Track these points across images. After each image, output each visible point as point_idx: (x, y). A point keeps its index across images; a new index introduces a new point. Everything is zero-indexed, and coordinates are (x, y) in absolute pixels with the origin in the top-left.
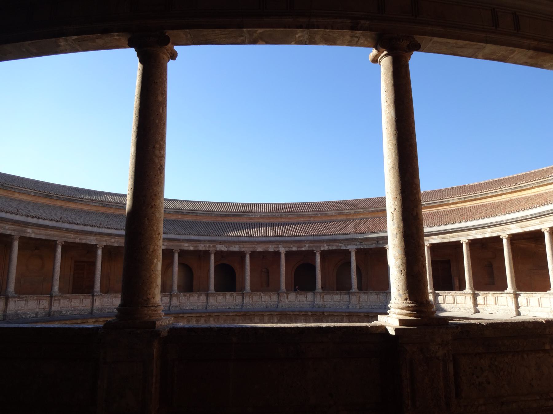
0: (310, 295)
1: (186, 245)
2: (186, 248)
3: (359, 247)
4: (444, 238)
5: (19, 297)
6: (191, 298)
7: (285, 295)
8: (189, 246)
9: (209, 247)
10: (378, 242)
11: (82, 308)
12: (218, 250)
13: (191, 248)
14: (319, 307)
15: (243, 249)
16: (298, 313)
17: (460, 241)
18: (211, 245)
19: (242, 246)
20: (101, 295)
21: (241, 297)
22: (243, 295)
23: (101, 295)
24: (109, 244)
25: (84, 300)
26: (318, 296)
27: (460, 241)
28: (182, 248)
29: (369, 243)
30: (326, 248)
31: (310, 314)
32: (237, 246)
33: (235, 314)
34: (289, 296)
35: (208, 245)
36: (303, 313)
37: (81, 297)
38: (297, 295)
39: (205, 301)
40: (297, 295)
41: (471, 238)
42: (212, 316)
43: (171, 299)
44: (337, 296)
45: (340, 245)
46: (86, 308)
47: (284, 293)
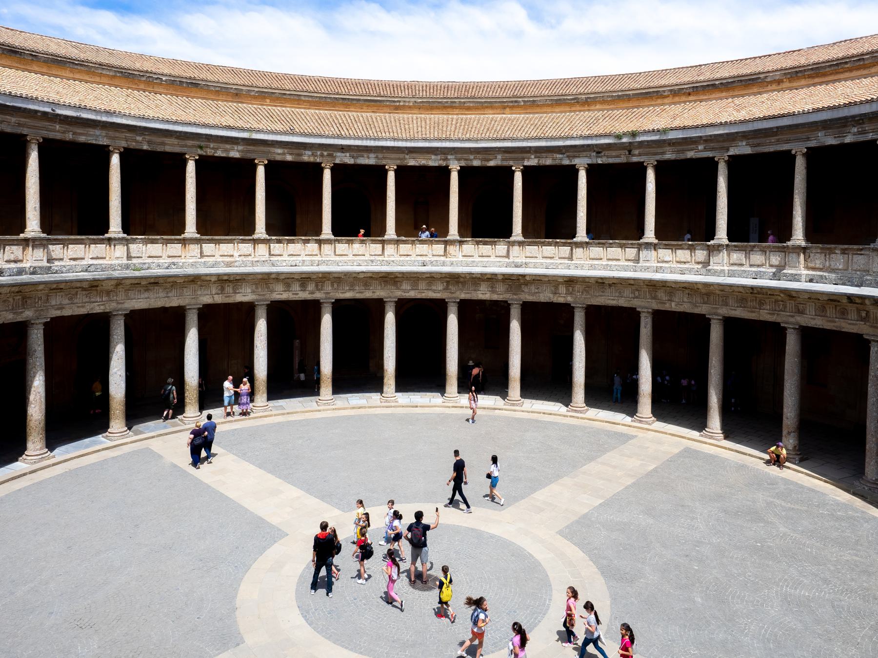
0: (501, 248)
1: (280, 151)
3: (595, 162)
4: (758, 145)
8: (284, 154)
9: (322, 155)
10: (630, 152)
12: (337, 161)
13: (289, 158)
14: (516, 266)
17: (790, 151)
18: (325, 153)
19: (380, 156)
24: (133, 145)
27: (790, 151)
28: (272, 158)
29: (614, 153)
32: (372, 155)
35: (319, 153)
41: (813, 144)
45: (561, 156)
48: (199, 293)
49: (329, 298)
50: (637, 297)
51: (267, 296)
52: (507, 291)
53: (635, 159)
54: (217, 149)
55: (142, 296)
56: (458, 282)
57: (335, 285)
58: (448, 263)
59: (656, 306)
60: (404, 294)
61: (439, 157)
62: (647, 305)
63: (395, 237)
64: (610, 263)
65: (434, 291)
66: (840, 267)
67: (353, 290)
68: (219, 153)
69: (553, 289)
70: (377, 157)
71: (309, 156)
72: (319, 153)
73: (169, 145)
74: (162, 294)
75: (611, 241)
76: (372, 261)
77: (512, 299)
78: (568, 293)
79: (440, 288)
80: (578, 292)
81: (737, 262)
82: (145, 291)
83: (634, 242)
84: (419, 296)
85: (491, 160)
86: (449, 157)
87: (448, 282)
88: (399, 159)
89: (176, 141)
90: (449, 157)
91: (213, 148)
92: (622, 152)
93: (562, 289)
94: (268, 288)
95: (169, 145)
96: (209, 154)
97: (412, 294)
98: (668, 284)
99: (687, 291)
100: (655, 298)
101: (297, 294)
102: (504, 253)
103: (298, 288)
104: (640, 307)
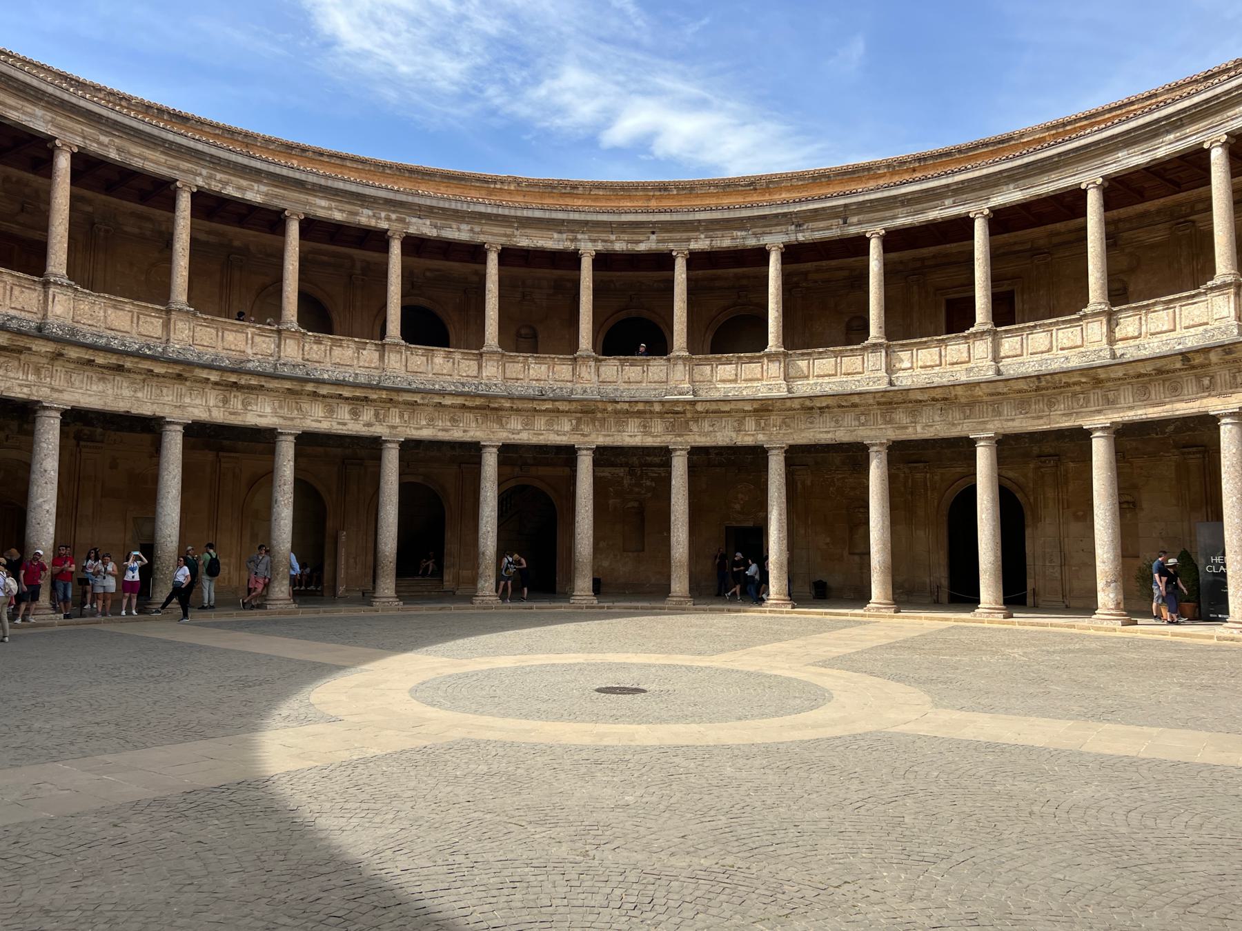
1: (323, 203)
2: (321, 213)
6: (337, 351)
7: (593, 364)
8: (330, 209)
11: (12, 313)
12: (412, 230)
13: (338, 216)
15: (481, 238)
16: (626, 406)
19: (477, 229)
21: (474, 364)
23: (69, 286)
25: (17, 291)
26: (680, 367)
29: (822, 224)
30: (701, 243)
32: (464, 227)
33: (460, 401)
34: (602, 369)
36: (640, 407)
39: (376, 363)
41: (1111, 169)
43: (279, 346)
44: (728, 367)
45: (744, 233)
46: (28, 316)
47: (589, 357)
48: (187, 400)
49: (395, 435)
50: (863, 425)
51: (297, 422)
53: (853, 230)
54: (227, 183)
55: (94, 388)
56: (593, 420)
57: (406, 417)
59: (892, 434)
60: (511, 436)
61: (564, 236)
62: (878, 433)
64: (820, 380)
66: (1165, 328)
68: (230, 191)
69: (736, 424)
70: (472, 230)
71: (369, 217)
72: (383, 214)
73: (152, 161)
74: (126, 393)
76: (463, 385)
77: (674, 443)
78: (760, 429)
79: (567, 428)
80: (774, 426)
81: (1011, 353)
82: (100, 380)
85: (641, 242)
86: (579, 236)
87: (579, 420)
88: (505, 235)
89: (162, 158)
90: (579, 236)
91: (220, 181)
92: (834, 222)
93: (750, 424)
95: (152, 161)
96: (213, 188)
97: (525, 437)
99: (939, 405)
100: (890, 422)
101: (345, 424)
102: (663, 376)
103: (347, 416)
104: (868, 437)
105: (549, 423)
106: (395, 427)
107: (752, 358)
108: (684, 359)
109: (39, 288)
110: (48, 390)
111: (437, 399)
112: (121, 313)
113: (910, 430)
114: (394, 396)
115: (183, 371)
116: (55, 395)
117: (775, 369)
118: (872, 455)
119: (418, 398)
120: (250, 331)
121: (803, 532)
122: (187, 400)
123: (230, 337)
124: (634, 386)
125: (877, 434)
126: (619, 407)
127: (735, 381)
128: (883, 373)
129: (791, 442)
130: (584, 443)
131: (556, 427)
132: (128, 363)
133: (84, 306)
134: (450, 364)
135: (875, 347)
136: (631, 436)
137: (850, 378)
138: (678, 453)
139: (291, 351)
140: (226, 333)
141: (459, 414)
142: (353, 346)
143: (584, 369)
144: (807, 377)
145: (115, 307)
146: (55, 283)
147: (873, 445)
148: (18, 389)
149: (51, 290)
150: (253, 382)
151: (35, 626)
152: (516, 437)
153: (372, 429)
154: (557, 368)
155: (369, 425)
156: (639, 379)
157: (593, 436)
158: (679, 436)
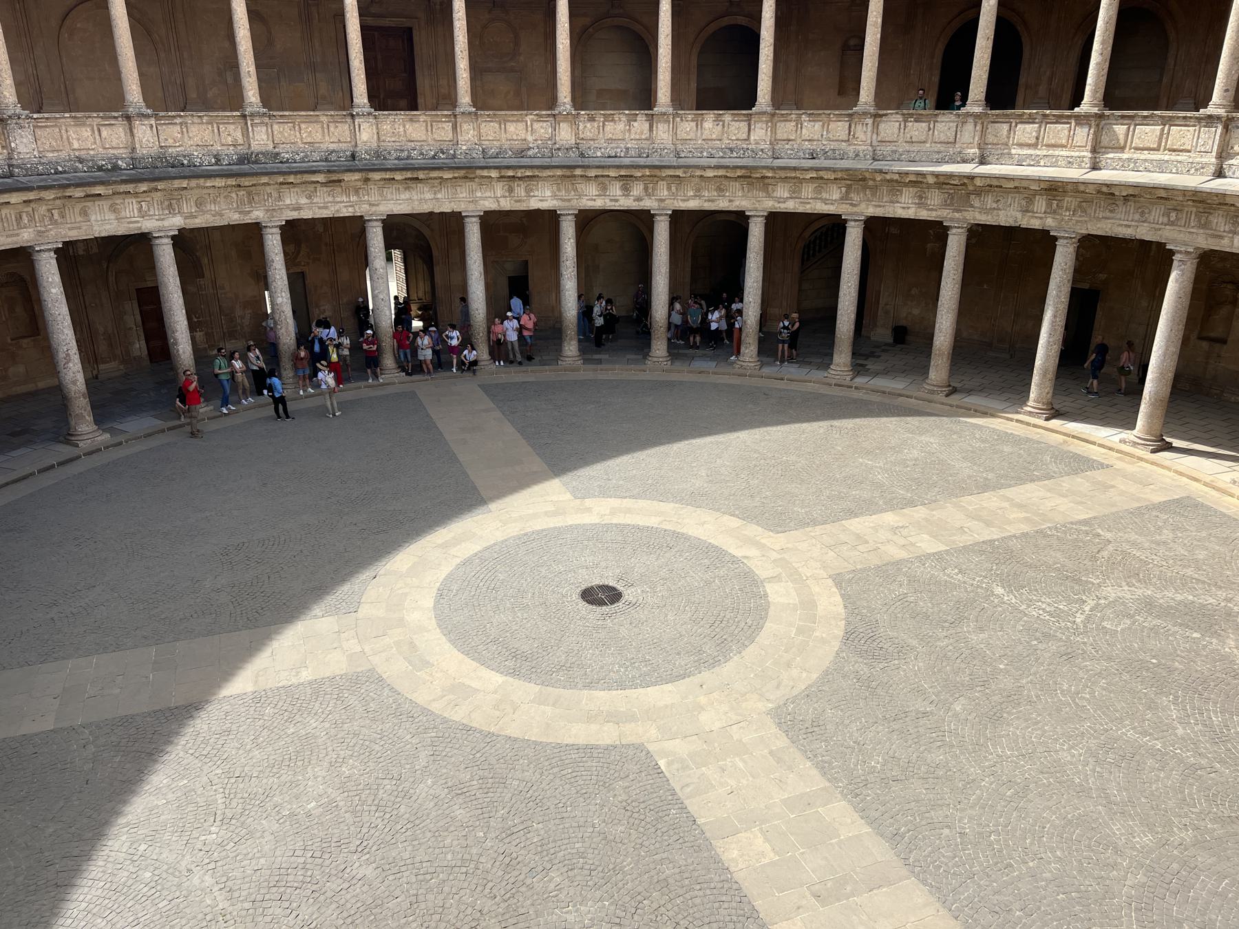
5: (157, 117)
6: (609, 126)
7: (870, 121)
11: (332, 146)
16: (896, 177)
20: (369, 114)
21: (744, 125)
22: (651, 118)
23: (369, 114)
26: (969, 127)
31: (931, 180)
33: (721, 172)
34: (882, 126)
37: (324, 119)
38: (905, 121)
39: (646, 135)
40: (905, 121)
42: (663, 179)
44: (1029, 127)
46: (343, 146)
50: (1172, 224)
51: (574, 203)
52: (945, 205)
55: (403, 196)
56: (865, 188)
57: (673, 188)
58: (851, 155)
59: (1205, 242)
60: (777, 205)
62: (1187, 238)
63: (769, 109)
65: (825, 201)
67: (700, 197)
74: (428, 196)
75: (1145, 113)
76: (731, 150)
77: (952, 220)
78: (1051, 211)
79: (836, 195)
80: (1068, 209)
83: (1189, 114)
84: (801, 209)
87: (849, 187)
93: (1040, 204)
94: (576, 190)
97: (791, 206)
98: (1229, 200)
100: (1205, 226)
101: (617, 201)
102: (951, 134)
103: (619, 192)
104: (1174, 241)
105: (818, 190)
106: (662, 200)
107: (1061, 116)
108: (976, 116)
109: (349, 120)
110: (367, 206)
111: (698, 173)
112: (417, 125)
113: (1226, 241)
114: (657, 172)
115: (467, 170)
116: (374, 209)
117: (1083, 135)
118: (1175, 264)
119: (679, 173)
120: (529, 118)
121: (1144, 304)
122: (479, 194)
123: (511, 127)
124: (915, 148)
125: (1186, 240)
126: (888, 177)
127: (1035, 146)
128: (1212, 159)
129: (1084, 232)
130: (852, 214)
131: (824, 195)
132: (421, 175)
133: (386, 127)
134: (720, 127)
135: (1211, 120)
136: (905, 207)
137: (1174, 157)
138: (954, 231)
139: (565, 134)
140: (508, 124)
141: (725, 182)
142: (624, 119)
143: (859, 127)
144: (1122, 149)
145: (411, 120)
146: (358, 114)
147: (1180, 252)
148: (344, 210)
149: (356, 121)
150: (528, 173)
151: (382, 385)
152: (782, 206)
153: (642, 204)
154: (832, 125)
155: (638, 199)
156: (923, 138)
157: (863, 205)
158: (960, 211)
